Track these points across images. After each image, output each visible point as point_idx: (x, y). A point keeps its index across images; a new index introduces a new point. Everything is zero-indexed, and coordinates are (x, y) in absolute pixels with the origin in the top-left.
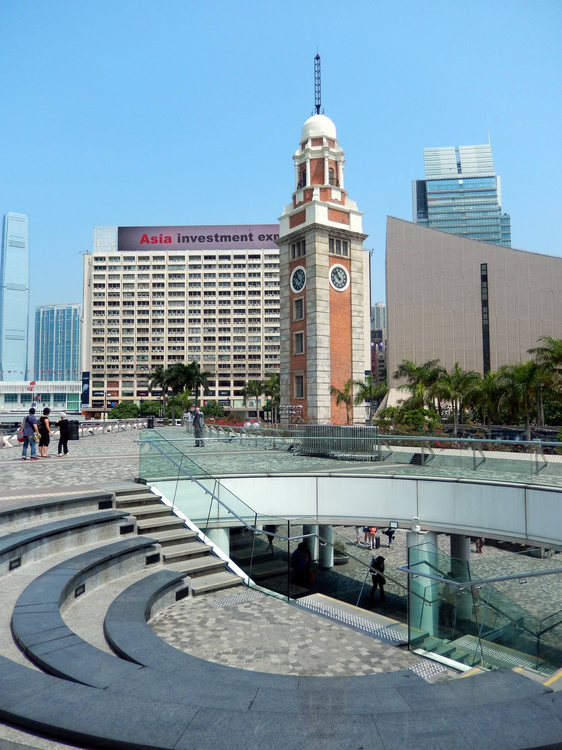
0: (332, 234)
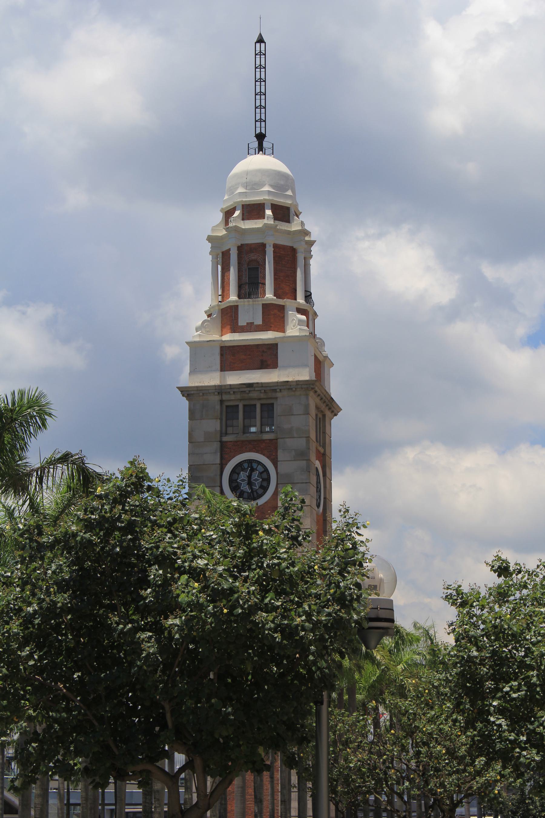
0: (225, 397)
